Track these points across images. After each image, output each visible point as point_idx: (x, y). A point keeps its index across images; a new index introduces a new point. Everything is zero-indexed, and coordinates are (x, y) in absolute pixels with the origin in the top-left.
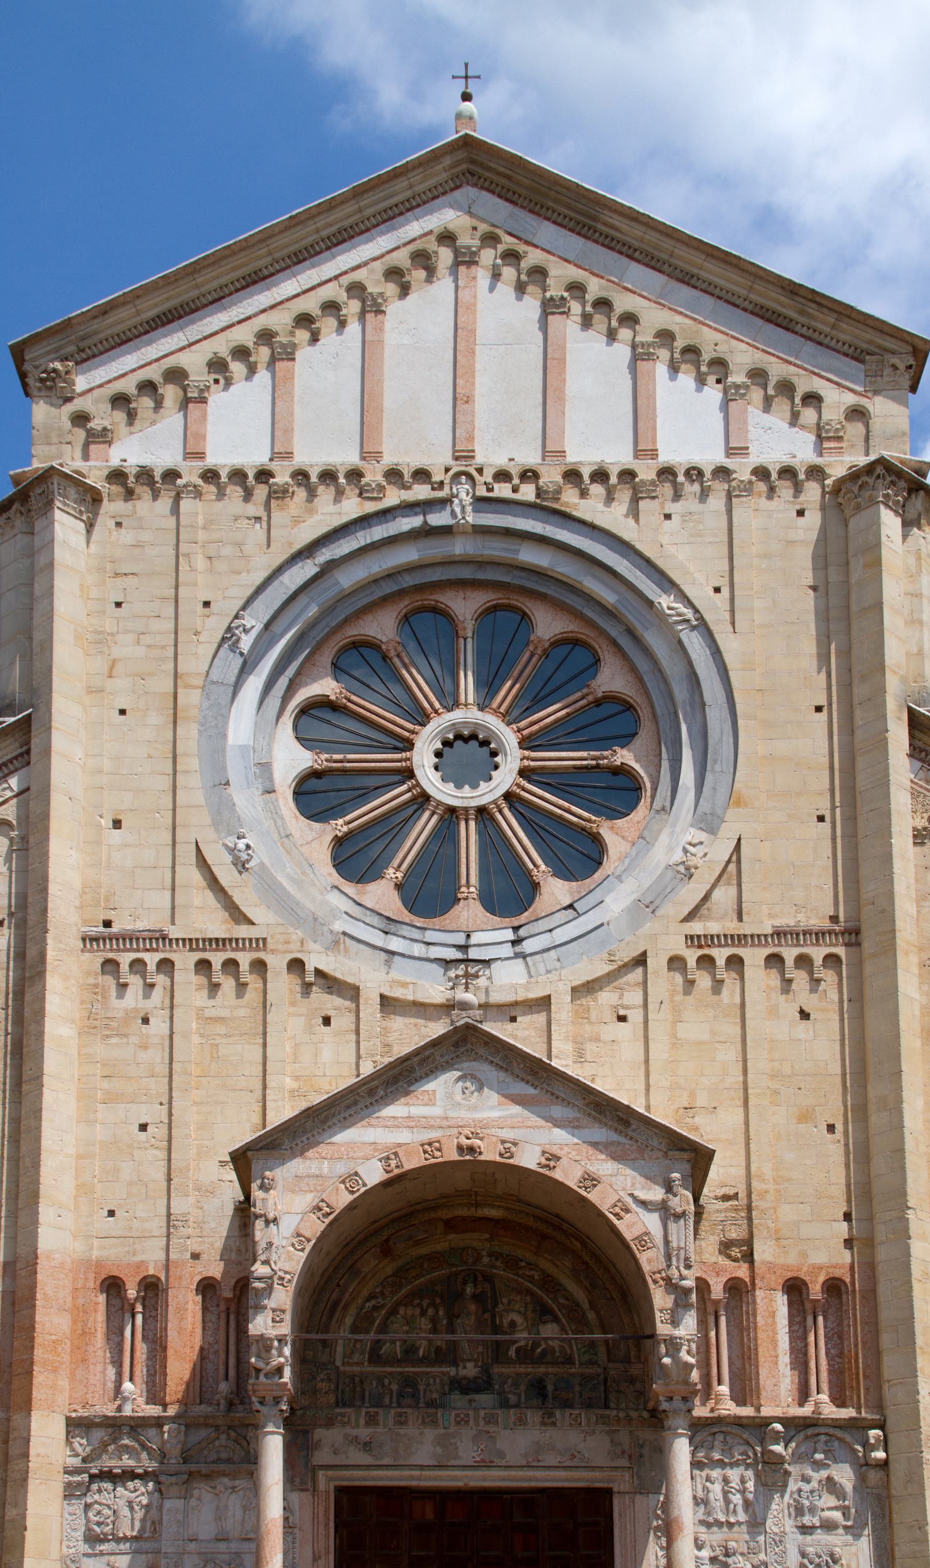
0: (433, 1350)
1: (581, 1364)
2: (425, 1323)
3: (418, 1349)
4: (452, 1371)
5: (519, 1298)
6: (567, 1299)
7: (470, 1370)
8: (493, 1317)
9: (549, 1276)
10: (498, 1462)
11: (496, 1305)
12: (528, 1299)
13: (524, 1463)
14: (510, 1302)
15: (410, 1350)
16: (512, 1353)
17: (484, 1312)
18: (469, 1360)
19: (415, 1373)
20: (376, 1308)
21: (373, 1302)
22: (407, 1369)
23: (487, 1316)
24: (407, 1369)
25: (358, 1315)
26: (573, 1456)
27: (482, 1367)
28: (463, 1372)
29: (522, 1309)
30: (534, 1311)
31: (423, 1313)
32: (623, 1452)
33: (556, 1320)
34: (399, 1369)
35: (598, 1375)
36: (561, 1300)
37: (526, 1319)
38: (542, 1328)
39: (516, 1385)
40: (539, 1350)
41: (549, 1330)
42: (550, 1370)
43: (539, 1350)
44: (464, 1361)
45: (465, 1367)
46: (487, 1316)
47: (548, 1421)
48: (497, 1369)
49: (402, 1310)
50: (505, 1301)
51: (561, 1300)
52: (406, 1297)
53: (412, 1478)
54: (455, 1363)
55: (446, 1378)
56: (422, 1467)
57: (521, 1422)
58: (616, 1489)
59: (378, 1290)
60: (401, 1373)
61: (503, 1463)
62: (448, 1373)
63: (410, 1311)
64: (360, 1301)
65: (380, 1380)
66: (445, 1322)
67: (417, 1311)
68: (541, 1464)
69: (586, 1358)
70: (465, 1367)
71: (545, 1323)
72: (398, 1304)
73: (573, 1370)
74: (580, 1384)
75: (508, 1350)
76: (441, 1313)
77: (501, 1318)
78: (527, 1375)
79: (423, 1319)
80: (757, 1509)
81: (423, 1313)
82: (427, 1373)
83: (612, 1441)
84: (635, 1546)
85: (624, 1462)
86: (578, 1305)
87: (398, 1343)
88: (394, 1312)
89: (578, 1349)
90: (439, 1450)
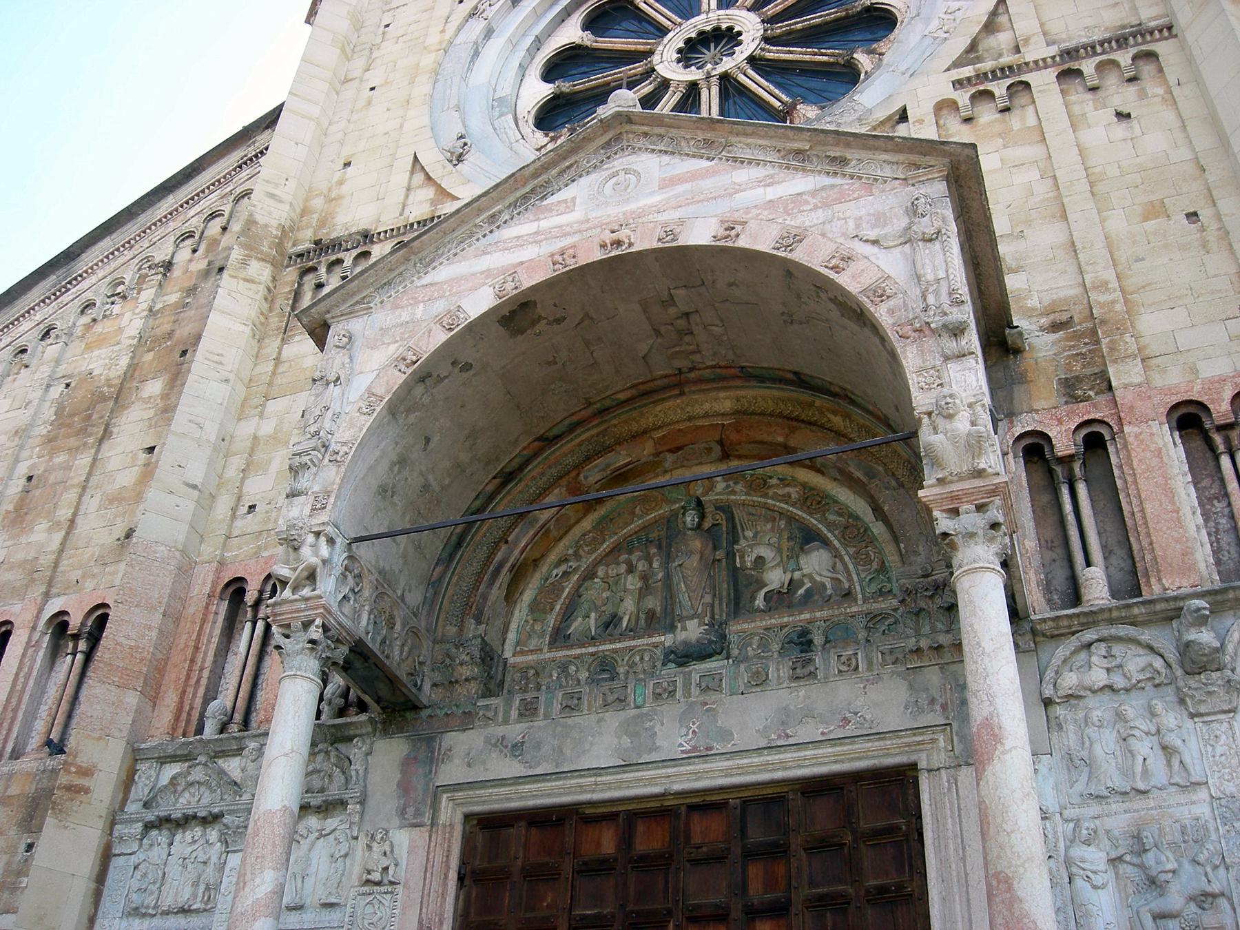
0: (642, 616)
1: (865, 600)
2: (632, 583)
3: (621, 619)
4: (667, 640)
5: (769, 526)
6: (840, 515)
7: (692, 631)
8: (730, 555)
9: (812, 489)
10: (718, 747)
11: (734, 539)
12: (783, 524)
13: (763, 743)
14: (755, 535)
15: (610, 624)
16: (760, 602)
17: (715, 548)
18: (692, 617)
19: (615, 651)
20: (566, 574)
21: (564, 567)
22: (601, 648)
23: (720, 554)
24: (601, 648)
25: (541, 590)
26: (846, 721)
27: (711, 625)
28: (681, 636)
29: (774, 540)
30: (790, 539)
31: (631, 569)
32: (932, 701)
33: (826, 543)
34: (591, 649)
35: (895, 610)
36: (832, 517)
37: (779, 550)
38: (803, 560)
39: (764, 645)
40: (801, 591)
41: (815, 564)
42: (818, 614)
43: (801, 591)
44: (682, 619)
45: (684, 629)
46: (720, 554)
47: (803, 672)
48: (736, 628)
49: (601, 571)
50: (749, 534)
51: (832, 517)
52: (607, 555)
53: (581, 789)
54: (672, 628)
55: (658, 651)
56: (598, 771)
57: (760, 681)
58: (922, 764)
59: (571, 552)
60: (593, 654)
61: (729, 747)
62: (662, 643)
63: (612, 571)
64: (544, 569)
65: (564, 668)
66: (660, 576)
67: (623, 568)
68: (791, 741)
69: (874, 587)
70: (684, 629)
71: (807, 553)
72: (597, 563)
73: (854, 609)
74: (867, 628)
75: (753, 598)
76: (656, 565)
77: (742, 557)
78: (782, 628)
79: (630, 577)
80: (1187, 760)
81: (631, 569)
82: (631, 649)
83: (911, 687)
84: (963, 859)
85: (934, 717)
86: (857, 518)
87: (593, 615)
88: (590, 575)
89: (861, 581)
90: (626, 741)
